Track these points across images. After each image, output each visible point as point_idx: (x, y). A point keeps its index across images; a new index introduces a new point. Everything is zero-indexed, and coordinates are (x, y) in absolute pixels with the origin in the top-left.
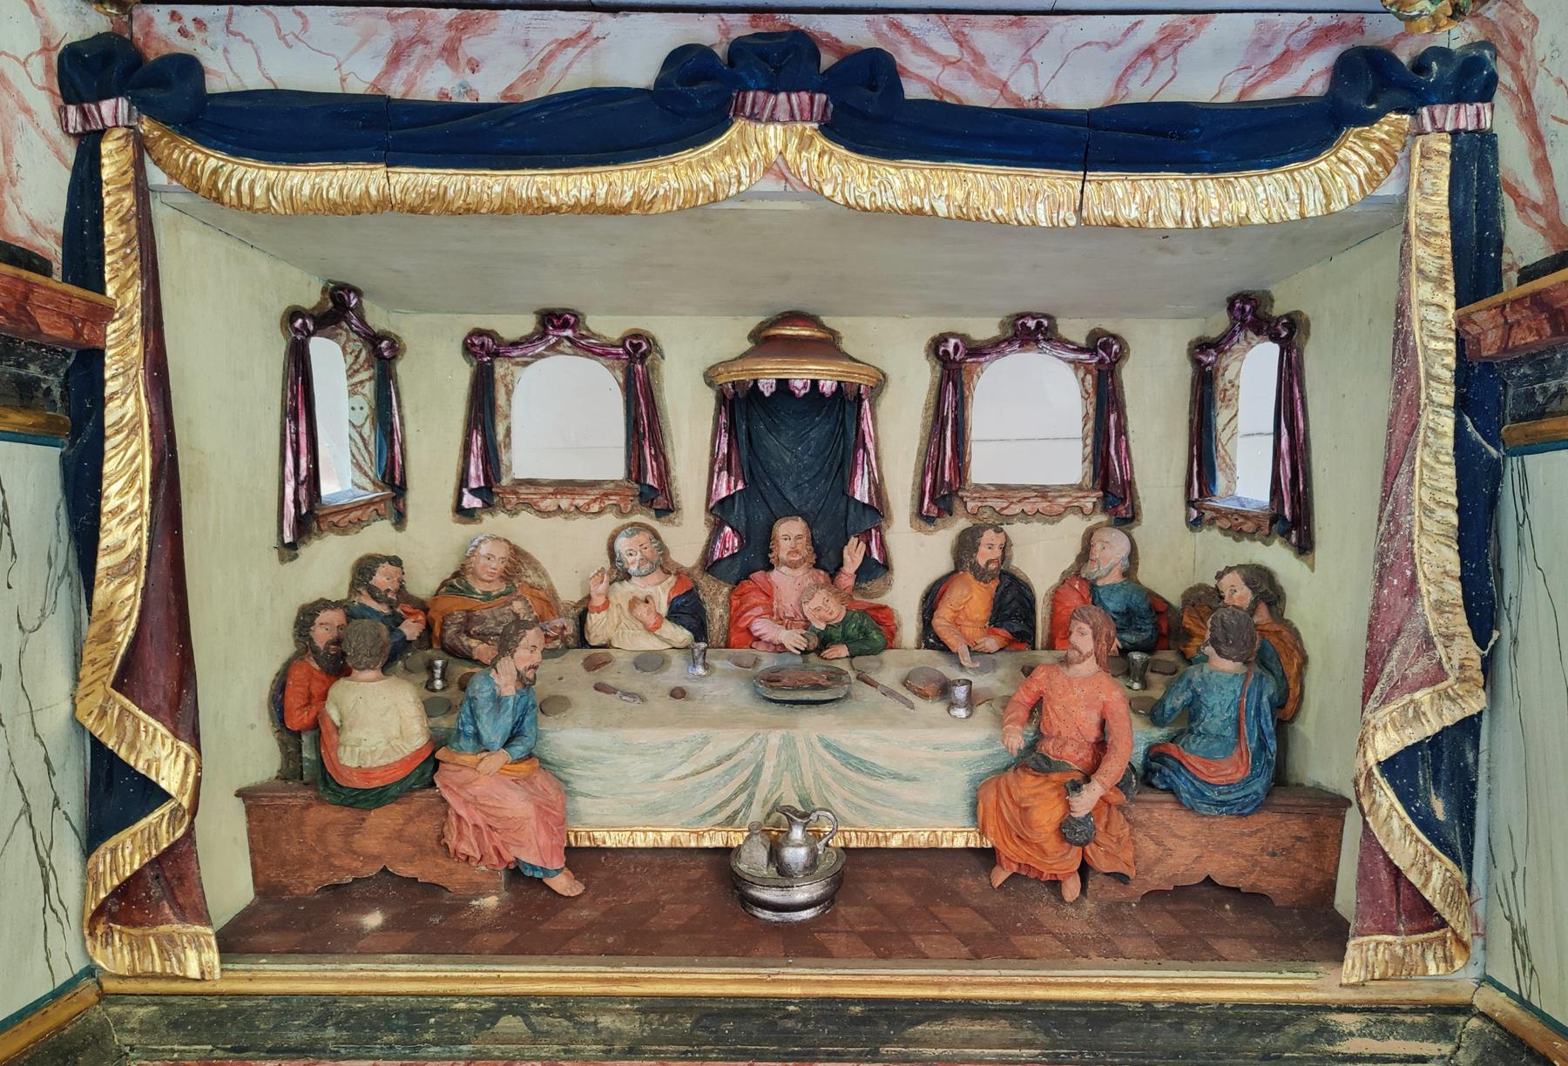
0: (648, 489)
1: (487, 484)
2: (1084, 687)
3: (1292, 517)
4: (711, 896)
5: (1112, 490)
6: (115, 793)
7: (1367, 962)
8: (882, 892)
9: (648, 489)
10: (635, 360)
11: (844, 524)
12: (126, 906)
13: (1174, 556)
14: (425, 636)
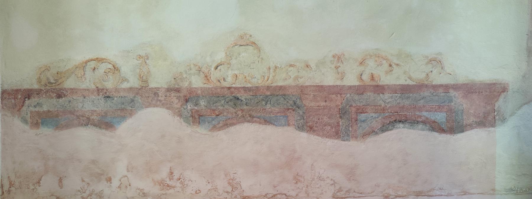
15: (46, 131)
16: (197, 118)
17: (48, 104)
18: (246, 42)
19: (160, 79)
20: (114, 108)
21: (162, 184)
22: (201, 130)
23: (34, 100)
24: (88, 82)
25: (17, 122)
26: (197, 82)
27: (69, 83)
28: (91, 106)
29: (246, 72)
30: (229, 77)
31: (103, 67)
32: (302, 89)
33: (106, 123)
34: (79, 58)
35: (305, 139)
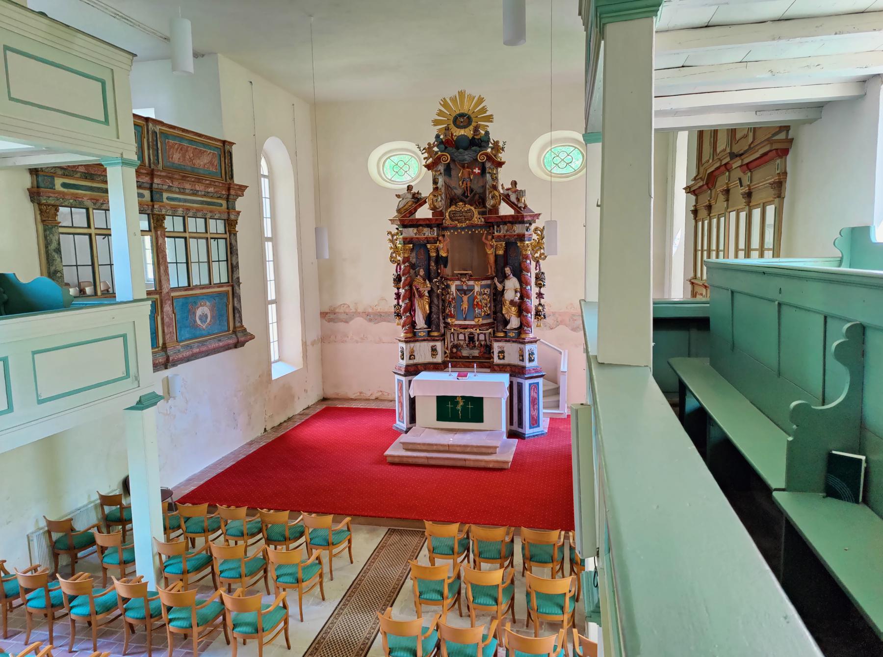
1: (458, 340)
4: (468, 358)
5: (485, 340)
6: (445, 353)
8: (474, 357)
11: (474, 342)
14: (456, 346)
15: (331, 323)
16: (370, 320)
17: (332, 316)
19: (360, 310)
22: (372, 324)
26: (370, 310)
33: (347, 322)
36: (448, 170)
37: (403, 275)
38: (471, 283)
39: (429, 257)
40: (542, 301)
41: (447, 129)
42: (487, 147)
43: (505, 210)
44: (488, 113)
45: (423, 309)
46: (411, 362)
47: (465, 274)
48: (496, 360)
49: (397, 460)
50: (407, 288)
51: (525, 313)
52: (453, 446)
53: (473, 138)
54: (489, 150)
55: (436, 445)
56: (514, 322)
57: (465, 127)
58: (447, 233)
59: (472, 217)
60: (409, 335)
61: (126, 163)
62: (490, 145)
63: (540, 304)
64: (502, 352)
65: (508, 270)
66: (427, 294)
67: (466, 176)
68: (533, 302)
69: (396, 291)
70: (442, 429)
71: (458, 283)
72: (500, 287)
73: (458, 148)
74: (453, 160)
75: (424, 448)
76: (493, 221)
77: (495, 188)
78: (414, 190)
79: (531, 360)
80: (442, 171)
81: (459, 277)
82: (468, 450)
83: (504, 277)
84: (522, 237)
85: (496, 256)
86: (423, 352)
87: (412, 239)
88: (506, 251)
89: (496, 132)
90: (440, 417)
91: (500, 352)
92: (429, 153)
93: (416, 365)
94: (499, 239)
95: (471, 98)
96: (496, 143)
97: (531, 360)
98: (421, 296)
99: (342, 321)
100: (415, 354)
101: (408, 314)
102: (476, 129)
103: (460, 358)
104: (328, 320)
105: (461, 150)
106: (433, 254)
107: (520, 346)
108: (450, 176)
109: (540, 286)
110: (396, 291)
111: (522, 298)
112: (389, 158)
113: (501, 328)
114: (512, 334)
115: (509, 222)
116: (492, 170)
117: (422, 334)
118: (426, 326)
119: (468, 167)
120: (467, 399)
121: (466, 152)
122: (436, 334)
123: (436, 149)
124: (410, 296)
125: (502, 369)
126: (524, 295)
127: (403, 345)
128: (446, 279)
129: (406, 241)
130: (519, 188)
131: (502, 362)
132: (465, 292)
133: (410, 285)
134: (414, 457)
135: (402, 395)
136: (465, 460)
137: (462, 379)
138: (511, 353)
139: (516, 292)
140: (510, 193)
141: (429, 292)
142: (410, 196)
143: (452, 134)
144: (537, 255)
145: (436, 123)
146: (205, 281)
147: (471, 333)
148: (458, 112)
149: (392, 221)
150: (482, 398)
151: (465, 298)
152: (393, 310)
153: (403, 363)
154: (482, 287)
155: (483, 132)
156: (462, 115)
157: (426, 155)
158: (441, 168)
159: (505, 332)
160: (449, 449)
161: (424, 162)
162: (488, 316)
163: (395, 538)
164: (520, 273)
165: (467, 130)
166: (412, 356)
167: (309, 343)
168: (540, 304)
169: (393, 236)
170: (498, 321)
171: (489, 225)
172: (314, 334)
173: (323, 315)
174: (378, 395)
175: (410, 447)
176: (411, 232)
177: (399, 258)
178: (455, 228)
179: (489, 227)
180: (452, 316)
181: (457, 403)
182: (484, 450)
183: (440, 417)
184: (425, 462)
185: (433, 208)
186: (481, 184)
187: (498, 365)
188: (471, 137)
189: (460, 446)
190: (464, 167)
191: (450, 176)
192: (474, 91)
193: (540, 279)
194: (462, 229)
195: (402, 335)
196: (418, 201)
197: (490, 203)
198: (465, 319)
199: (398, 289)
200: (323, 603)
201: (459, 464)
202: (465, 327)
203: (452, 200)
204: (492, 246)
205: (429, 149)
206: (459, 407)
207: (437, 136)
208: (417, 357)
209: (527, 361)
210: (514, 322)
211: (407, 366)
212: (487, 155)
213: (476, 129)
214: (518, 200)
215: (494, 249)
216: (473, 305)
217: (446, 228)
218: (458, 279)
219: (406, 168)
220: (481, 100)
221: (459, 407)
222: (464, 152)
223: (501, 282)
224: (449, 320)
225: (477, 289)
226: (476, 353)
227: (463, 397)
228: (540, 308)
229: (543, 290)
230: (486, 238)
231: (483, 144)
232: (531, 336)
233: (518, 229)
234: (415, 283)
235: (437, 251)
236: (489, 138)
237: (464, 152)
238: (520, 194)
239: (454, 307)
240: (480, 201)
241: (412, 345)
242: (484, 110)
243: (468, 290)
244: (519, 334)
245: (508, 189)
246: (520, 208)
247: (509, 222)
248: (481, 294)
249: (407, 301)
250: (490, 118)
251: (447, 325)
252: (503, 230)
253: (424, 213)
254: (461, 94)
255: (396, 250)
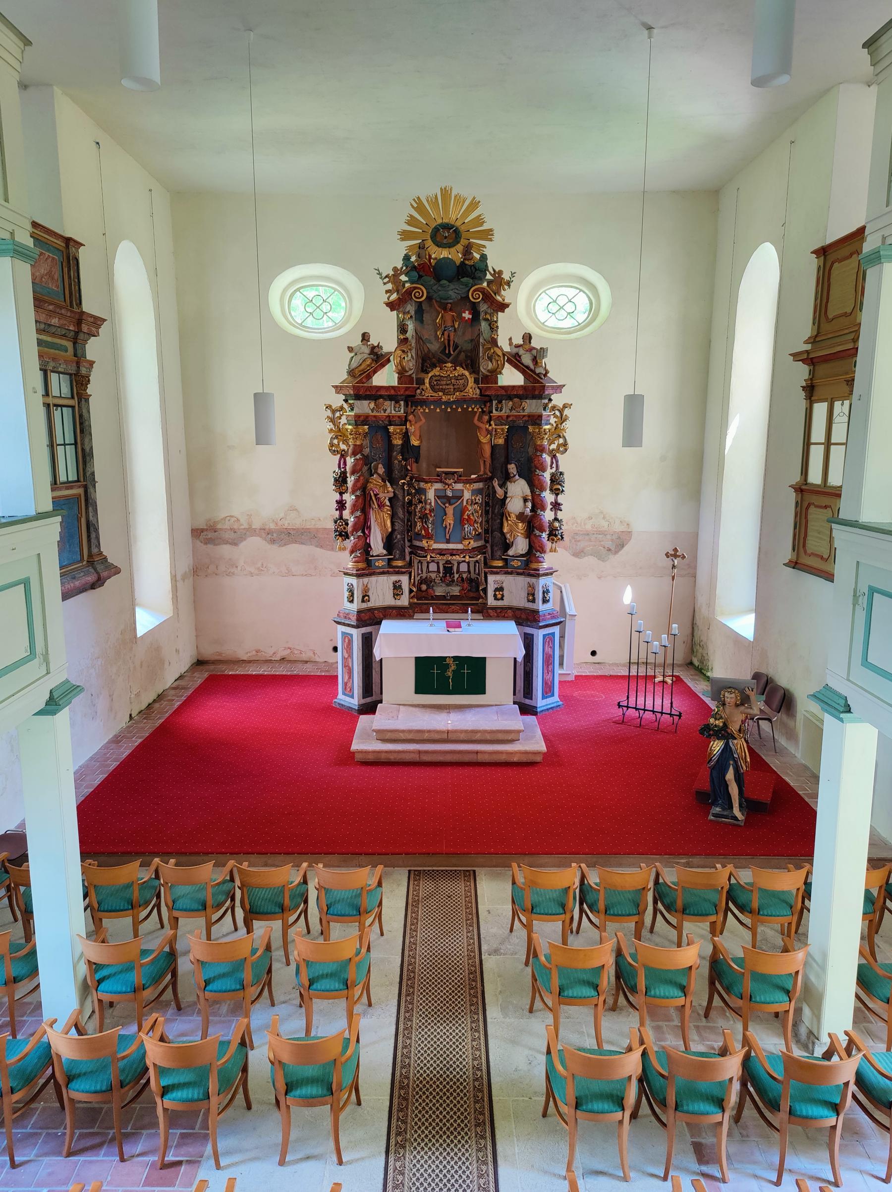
0: (438, 571)
2: (466, 585)
3: (479, 574)
4: (443, 598)
5: (469, 571)
7: (480, 600)
8: (454, 597)
9: (438, 571)
10: (438, 563)
12: (412, 598)
13: (473, 576)
15: (210, 546)
16: (273, 541)
17: (210, 535)
18: (293, 509)
19: (256, 525)
20: (237, 537)
21: (258, 569)
22: (275, 547)
23: (205, 533)
24: (226, 527)
25: (198, 542)
26: (272, 526)
27: (219, 526)
28: (228, 535)
29: (293, 522)
30: (286, 524)
31: (233, 519)
32: (318, 530)
33: (236, 544)
34: (223, 516)
35: (319, 550)
36: (420, 312)
37: (353, 473)
38: (459, 486)
39: (390, 446)
40: (560, 515)
41: (421, 247)
42: (482, 279)
43: (511, 377)
44: (485, 227)
45: (383, 526)
46: (364, 606)
47: (453, 473)
48: (491, 601)
49: (371, 758)
50: (358, 493)
51: (537, 532)
52: (455, 731)
53: (462, 263)
54: (485, 284)
55: (429, 731)
56: (520, 545)
57: (450, 246)
58: (420, 410)
59: (465, 386)
60: (361, 565)
61: (18, 252)
62: (489, 277)
63: (556, 519)
64: (501, 589)
65: (512, 468)
66: (388, 503)
67: (449, 323)
68: (548, 515)
69: (337, 497)
70: (424, 706)
71: (438, 486)
72: (500, 492)
73: (438, 279)
74: (429, 298)
75: (410, 736)
76: (491, 395)
77: (494, 342)
78: (373, 341)
79: (545, 601)
80: (413, 313)
81: (440, 478)
82: (478, 736)
83: (506, 478)
84: (537, 420)
85: (494, 448)
86: (381, 590)
87: (367, 417)
88: (506, 440)
89: (497, 256)
90: (419, 690)
91: (496, 590)
92: (394, 283)
93: (371, 610)
94: (500, 420)
95: (459, 200)
96: (498, 274)
97: (545, 601)
98: (381, 506)
99: (227, 542)
100: (370, 594)
101: (360, 533)
102: (467, 251)
103: (433, 598)
104: (205, 539)
105: (444, 282)
106: (398, 442)
107: (528, 579)
108: (422, 321)
109: (557, 492)
110: (337, 497)
111: (533, 510)
112: (298, 290)
113: (499, 553)
114: (516, 563)
115: (517, 396)
116: (491, 315)
117: (380, 564)
118: (385, 552)
119: (451, 310)
120: (461, 661)
121: (452, 286)
122: (399, 563)
123: (403, 278)
124: (364, 504)
125: (501, 614)
126: (537, 505)
127: (354, 581)
128: (420, 480)
129: (360, 420)
130: (535, 343)
131: (499, 603)
132: (449, 500)
133: (364, 489)
134: (399, 752)
135: (351, 655)
136: (477, 752)
137: (456, 632)
138: (514, 589)
139: (525, 500)
140: (521, 351)
141: (390, 500)
142: (367, 350)
143: (430, 256)
144: (553, 446)
145: (405, 236)
146: (66, 480)
147: (448, 562)
148: (439, 221)
149: (338, 389)
150: (484, 660)
151: (450, 510)
152: (331, 526)
153: (354, 607)
154: (475, 492)
155: (477, 256)
156: (446, 227)
157: (390, 286)
158: (411, 308)
159: (506, 560)
160: (447, 737)
161: (385, 298)
162: (478, 536)
163: (425, 887)
164: (530, 473)
165: (453, 250)
166: (365, 598)
167: (179, 577)
168: (556, 519)
169: (334, 412)
170: (494, 542)
171: (485, 399)
172: (185, 564)
173: (197, 533)
174: (285, 653)
175: (388, 736)
176: (365, 407)
177: (343, 447)
178: (438, 402)
179: (485, 403)
180: (429, 537)
181: (447, 666)
182: (500, 736)
183: (419, 690)
184: (416, 758)
185: (401, 372)
186: (468, 337)
187: (494, 609)
188: (458, 263)
189: (466, 731)
190: (445, 309)
191: (422, 321)
192: (463, 189)
193: (557, 481)
194: (448, 404)
195: (350, 565)
196: (378, 358)
197: (485, 366)
198: (448, 542)
199: (341, 494)
200: (370, 1010)
201: (466, 758)
202: (441, 552)
203: (426, 362)
204: (489, 432)
205: (394, 278)
206: (450, 673)
207: (407, 258)
208: (372, 599)
209: (541, 602)
210: (520, 545)
211: (359, 612)
212: (483, 291)
213: (467, 251)
214: (535, 360)
215: (490, 436)
216: (461, 520)
217: (423, 403)
218: (441, 481)
219: (325, 307)
220: (474, 205)
221: (450, 673)
222: (447, 284)
223: (501, 486)
224: (417, 543)
225: (467, 495)
226: (456, 590)
227: (456, 658)
228: (557, 524)
229: (561, 498)
230: (480, 419)
231: (478, 274)
232: (545, 565)
233: (530, 406)
234: (370, 486)
235: (406, 436)
236: (487, 266)
237: (447, 284)
238: (538, 355)
239: (433, 523)
240: (472, 365)
241: (366, 580)
242: (479, 221)
243: (453, 497)
244: (527, 564)
245: (517, 346)
246: (538, 375)
247: (517, 396)
248: (473, 503)
249: (358, 513)
250: (488, 235)
251: (415, 550)
252: (506, 408)
253: (386, 377)
254: (445, 193)
255: (339, 434)
